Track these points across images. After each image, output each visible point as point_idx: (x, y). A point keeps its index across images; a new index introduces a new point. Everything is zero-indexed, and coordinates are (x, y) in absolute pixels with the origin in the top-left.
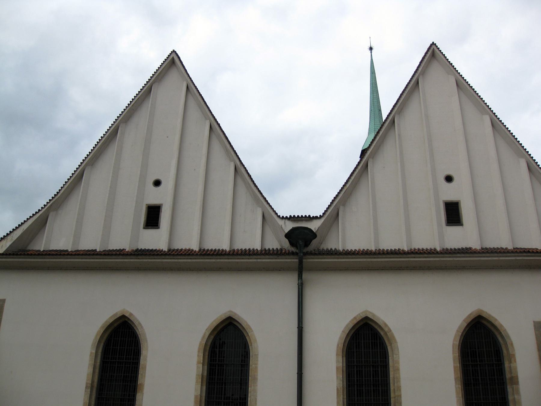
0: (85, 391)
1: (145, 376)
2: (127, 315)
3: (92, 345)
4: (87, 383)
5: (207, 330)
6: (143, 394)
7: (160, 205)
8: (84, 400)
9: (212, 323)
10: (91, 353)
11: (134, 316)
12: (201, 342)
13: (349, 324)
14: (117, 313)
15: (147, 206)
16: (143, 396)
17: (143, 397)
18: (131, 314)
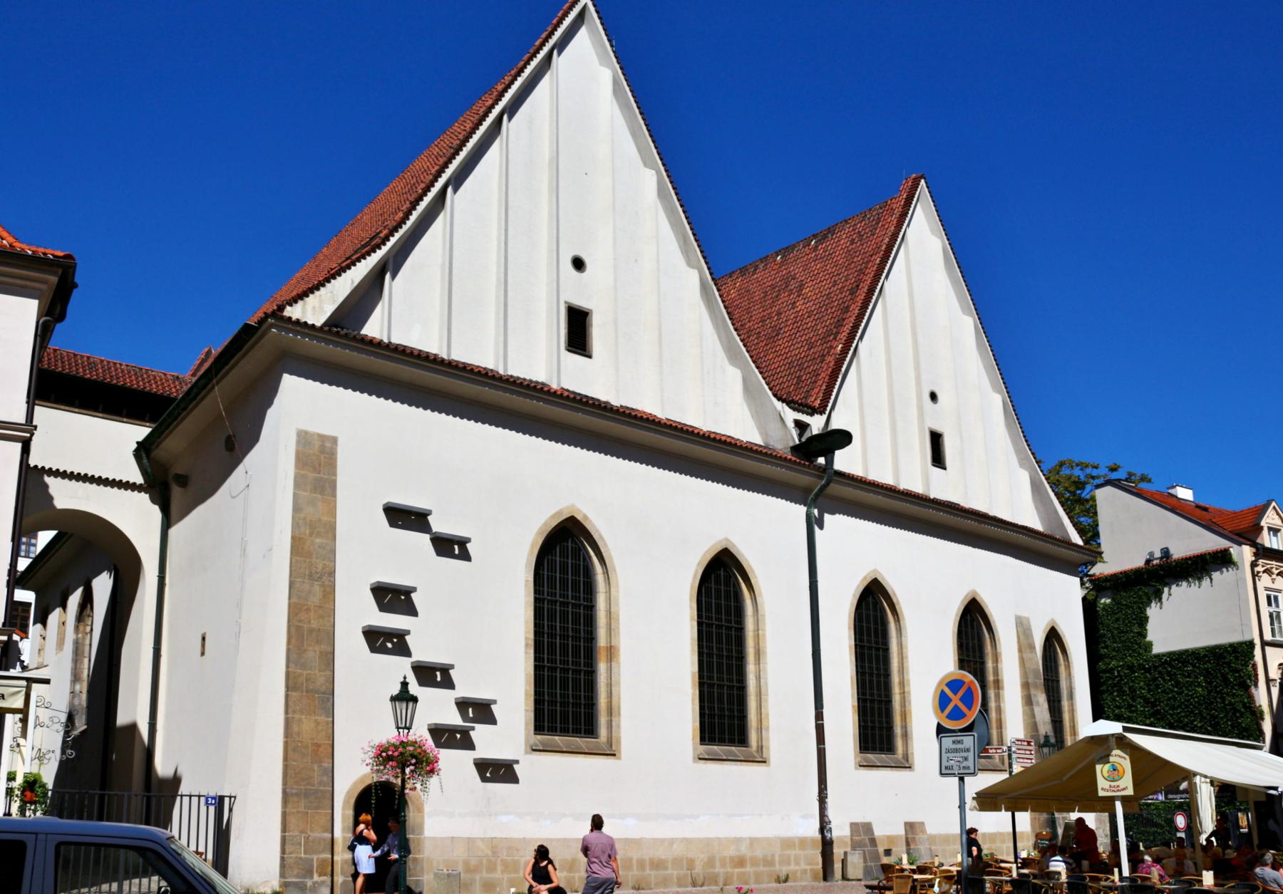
0: (526, 653)
1: (619, 632)
2: (579, 517)
3: (526, 567)
4: (526, 639)
5: (698, 564)
6: (618, 663)
7: (588, 311)
8: (525, 668)
9: (704, 555)
10: (527, 581)
11: (591, 521)
12: (692, 584)
13: (859, 585)
14: (561, 510)
15: (567, 305)
16: (619, 668)
17: (619, 672)
18: (586, 517)
